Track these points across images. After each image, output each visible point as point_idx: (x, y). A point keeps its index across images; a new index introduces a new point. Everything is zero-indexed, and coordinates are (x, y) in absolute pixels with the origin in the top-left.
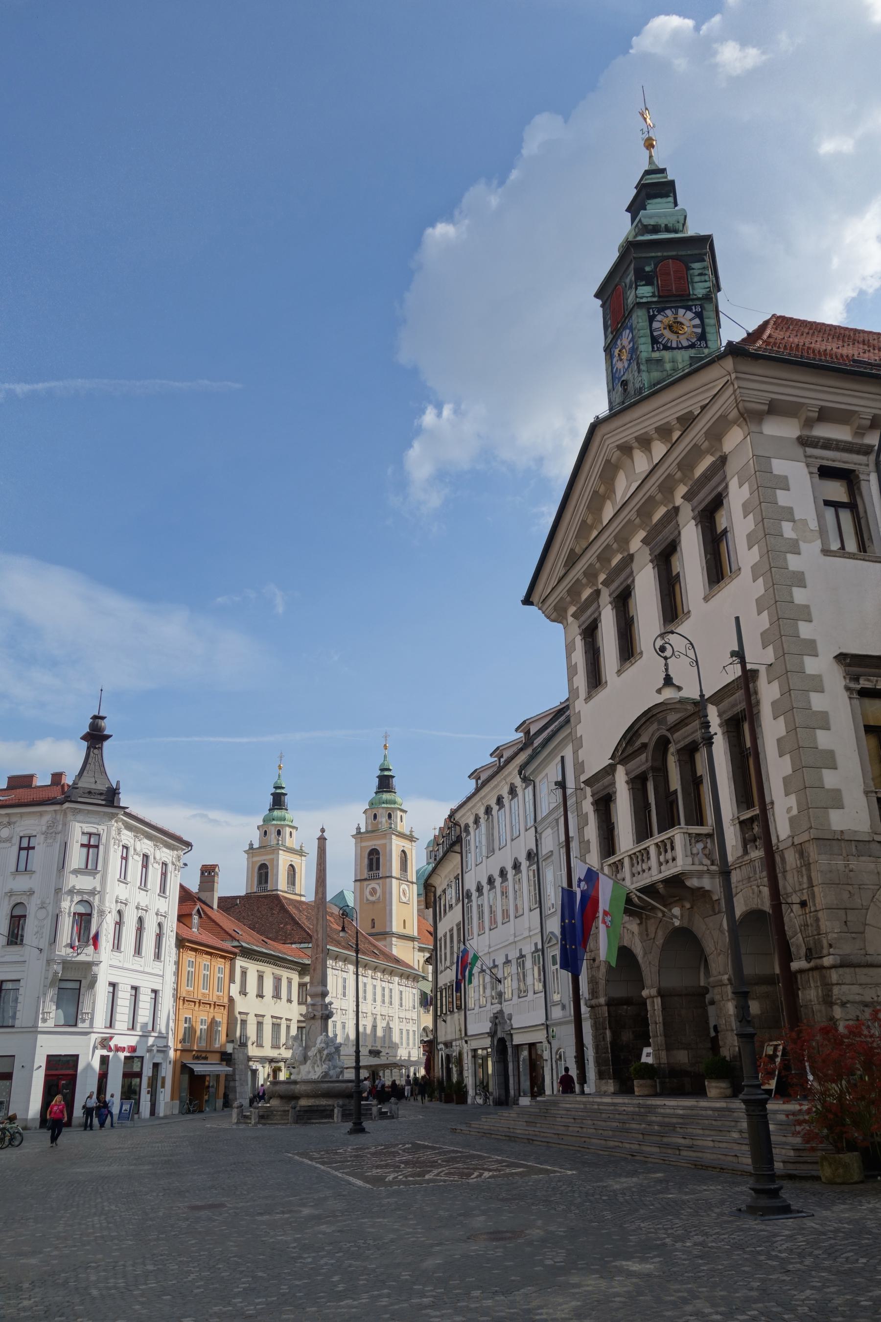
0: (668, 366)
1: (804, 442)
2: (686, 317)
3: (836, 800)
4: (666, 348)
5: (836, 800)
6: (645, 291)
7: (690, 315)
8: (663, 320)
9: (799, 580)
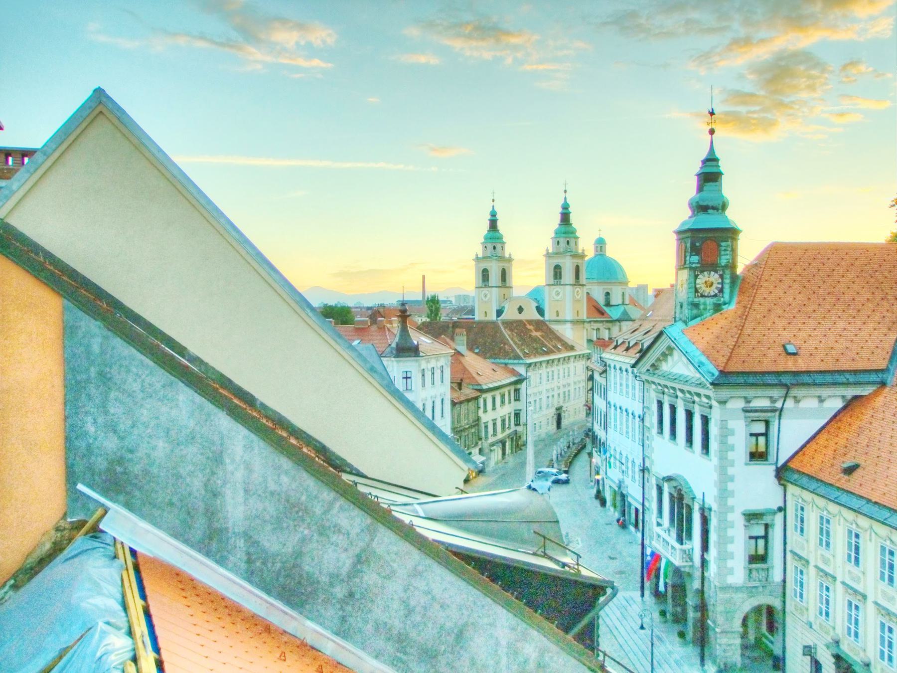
0: (702, 307)
1: (745, 411)
2: (714, 277)
3: (731, 571)
4: (702, 296)
5: (731, 571)
6: (695, 259)
7: (717, 276)
8: (701, 280)
9: (732, 479)
